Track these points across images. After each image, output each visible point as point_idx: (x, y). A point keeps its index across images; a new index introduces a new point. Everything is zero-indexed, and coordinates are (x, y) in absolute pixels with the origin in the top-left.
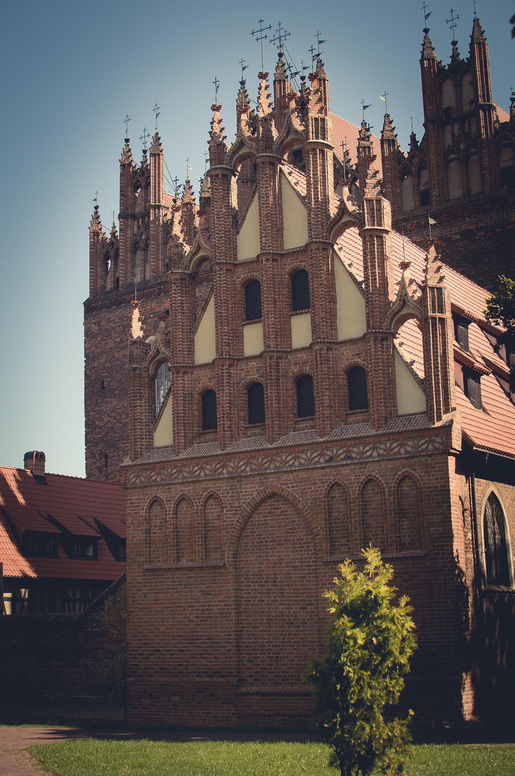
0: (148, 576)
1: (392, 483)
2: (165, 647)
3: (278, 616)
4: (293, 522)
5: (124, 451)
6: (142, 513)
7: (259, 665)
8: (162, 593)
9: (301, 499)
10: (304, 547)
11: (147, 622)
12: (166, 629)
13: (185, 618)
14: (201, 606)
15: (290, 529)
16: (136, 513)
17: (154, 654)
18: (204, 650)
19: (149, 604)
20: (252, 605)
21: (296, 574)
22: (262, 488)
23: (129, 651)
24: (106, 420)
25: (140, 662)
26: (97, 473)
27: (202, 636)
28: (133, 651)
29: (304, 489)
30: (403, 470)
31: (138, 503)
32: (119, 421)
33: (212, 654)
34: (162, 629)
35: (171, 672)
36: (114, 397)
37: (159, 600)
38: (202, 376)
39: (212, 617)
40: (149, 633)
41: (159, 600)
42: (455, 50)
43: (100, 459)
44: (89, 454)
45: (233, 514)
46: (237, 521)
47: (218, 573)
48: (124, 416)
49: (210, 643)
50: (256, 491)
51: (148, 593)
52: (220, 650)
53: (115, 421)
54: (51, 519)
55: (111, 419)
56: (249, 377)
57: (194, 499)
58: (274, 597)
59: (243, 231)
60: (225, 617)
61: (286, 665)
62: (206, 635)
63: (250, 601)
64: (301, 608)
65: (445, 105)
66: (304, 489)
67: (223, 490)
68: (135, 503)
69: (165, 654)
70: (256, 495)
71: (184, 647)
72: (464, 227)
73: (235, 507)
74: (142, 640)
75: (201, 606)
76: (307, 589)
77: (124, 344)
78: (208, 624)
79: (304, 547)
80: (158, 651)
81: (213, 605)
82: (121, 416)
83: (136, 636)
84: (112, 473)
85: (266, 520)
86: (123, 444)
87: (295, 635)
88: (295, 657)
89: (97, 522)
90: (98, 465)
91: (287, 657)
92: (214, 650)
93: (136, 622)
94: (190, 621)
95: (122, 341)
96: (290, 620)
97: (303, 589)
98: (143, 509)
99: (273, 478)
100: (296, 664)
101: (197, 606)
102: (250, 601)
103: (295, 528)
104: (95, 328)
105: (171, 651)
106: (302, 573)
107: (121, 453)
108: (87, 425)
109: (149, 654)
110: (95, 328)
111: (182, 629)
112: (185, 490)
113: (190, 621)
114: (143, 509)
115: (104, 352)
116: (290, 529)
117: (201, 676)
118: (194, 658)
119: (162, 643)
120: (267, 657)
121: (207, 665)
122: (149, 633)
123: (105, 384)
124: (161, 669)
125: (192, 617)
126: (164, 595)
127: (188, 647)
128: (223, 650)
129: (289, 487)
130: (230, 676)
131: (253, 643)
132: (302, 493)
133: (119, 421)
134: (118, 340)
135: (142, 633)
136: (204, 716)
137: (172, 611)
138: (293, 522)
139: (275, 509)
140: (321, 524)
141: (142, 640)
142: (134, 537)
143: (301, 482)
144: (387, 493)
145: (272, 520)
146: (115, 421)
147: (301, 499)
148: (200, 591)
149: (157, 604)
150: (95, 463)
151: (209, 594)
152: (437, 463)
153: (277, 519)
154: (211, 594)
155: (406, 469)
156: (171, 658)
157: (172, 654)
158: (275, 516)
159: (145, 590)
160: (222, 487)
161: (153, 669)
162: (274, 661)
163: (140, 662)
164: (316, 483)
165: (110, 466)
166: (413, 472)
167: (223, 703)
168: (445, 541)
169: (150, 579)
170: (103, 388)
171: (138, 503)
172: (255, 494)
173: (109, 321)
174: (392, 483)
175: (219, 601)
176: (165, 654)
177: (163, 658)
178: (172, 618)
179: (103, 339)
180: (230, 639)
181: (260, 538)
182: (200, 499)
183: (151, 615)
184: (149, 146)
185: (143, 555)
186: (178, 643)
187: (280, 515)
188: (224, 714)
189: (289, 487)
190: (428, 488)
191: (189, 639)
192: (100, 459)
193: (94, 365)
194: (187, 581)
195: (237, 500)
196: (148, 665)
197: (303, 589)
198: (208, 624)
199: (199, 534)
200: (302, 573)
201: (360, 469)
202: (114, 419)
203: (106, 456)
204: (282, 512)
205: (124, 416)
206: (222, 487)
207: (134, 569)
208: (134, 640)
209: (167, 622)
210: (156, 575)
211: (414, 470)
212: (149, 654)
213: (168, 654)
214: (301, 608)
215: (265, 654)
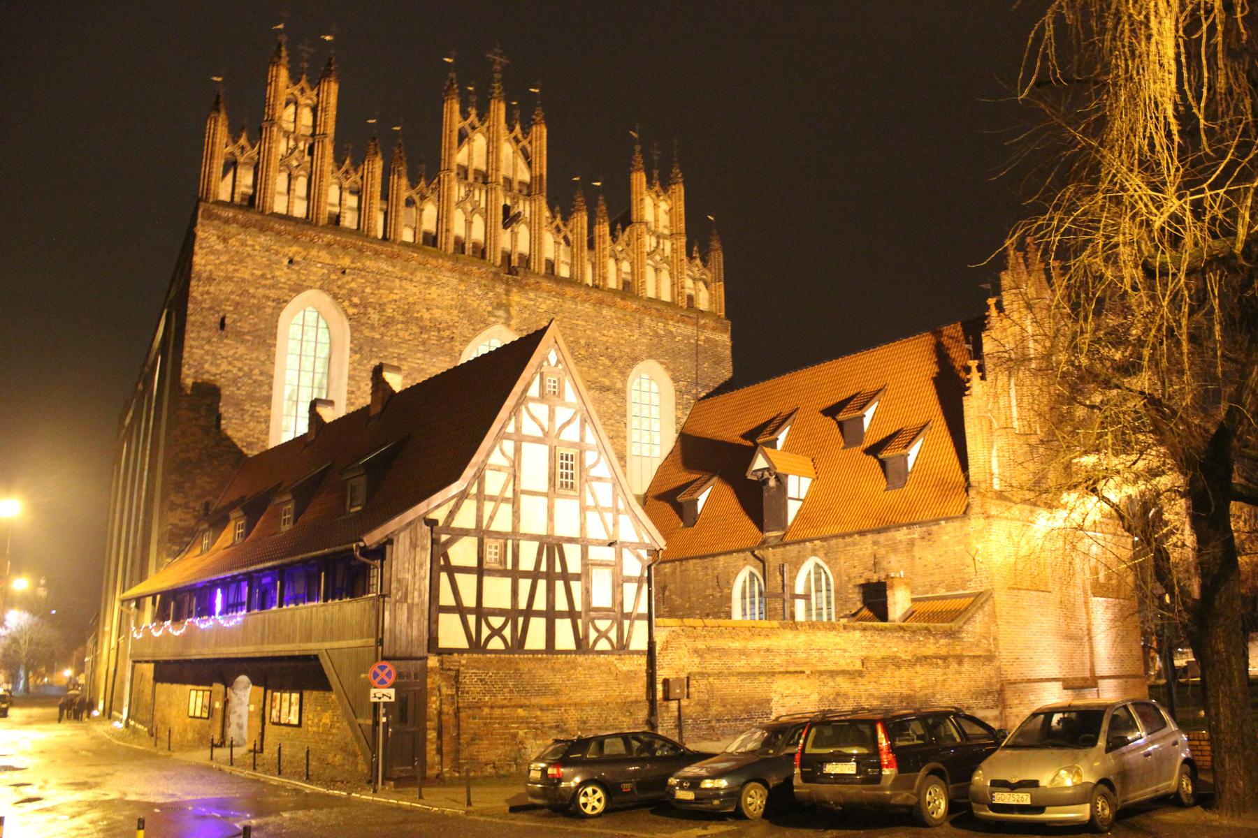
5: (252, 415)
24: (224, 367)
53: (241, 374)
77: (268, 282)
82: (251, 370)
95: (263, 276)
115: (231, 279)
123: (227, 321)
133: (249, 375)
134: (258, 273)
170: (222, 325)
173: (243, 244)
179: (228, 262)
205: (256, 371)
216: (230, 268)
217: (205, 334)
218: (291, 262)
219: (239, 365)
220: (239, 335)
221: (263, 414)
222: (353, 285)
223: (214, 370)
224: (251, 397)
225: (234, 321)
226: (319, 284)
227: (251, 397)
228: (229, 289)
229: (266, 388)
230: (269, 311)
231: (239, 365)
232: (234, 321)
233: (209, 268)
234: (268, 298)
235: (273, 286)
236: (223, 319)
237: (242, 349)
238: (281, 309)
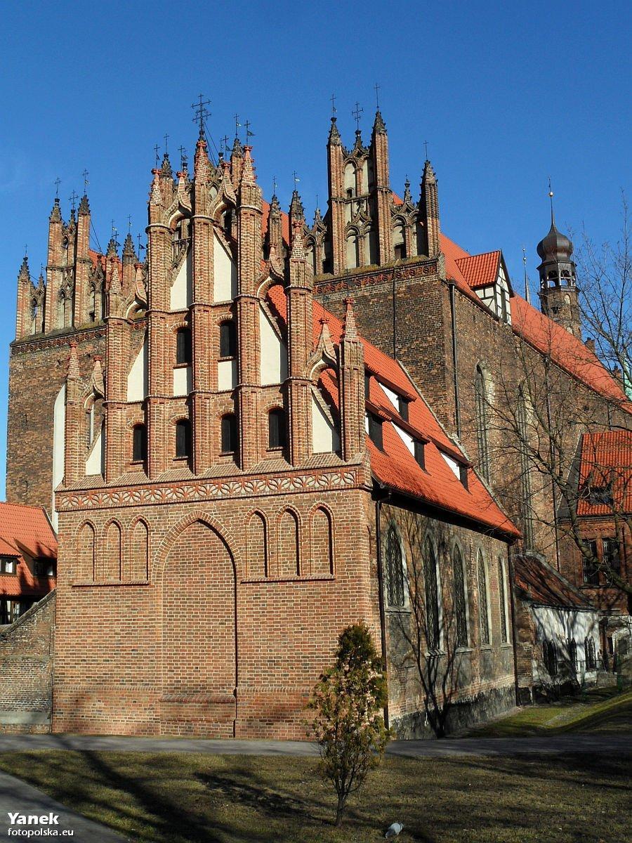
0: (77, 592)
1: (307, 513)
2: (92, 657)
3: (199, 630)
4: (214, 545)
6: (74, 534)
7: (180, 674)
8: (90, 607)
9: (223, 525)
10: (224, 568)
11: (75, 634)
12: (93, 641)
13: (111, 630)
14: (126, 620)
15: (212, 552)
16: (67, 534)
17: (80, 664)
18: (129, 661)
19: (77, 617)
20: (175, 620)
21: (217, 592)
22: (187, 515)
23: (56, 660)
24: (27, 450)
25: (66, 670)
26: (16, 497)
27: (127, 647)
28: (60, 660)
29: (226, 516)
30: (318, 502)
31: (70, 525)
32: (40, 451)
33: (136, 664)
34: (89, 640)
35: (97, 681)
36: (36, 430)
37: (87, 614)
38: (134, 412)
39: (136, 630)
40: (76, 644)
41: (87, 614)
42: (358, 139)
43: (20, 486)
44: (9, 481)
45: (160, 537)
46: (163, 543)
47: (144, 590)
49: (134, 654)
50: (182, 517)
51: (76, 608)
52: (143, 661)
53: (36, 452)
54: (421, 490)
55: (33, 450)
56: (177, 415)
57: (124, 523)
58: (195, 613)
59: (175, 283)
60: (149, 630)
61: (205, 675)
62: (131, 647)
63: (173, 616)
64: (220, 624)
65: (347, 187)
66: (226, 516)
67: (151, 515)
68: (67, 525)
69: (91, 664)
70: (181, 521)
71: (109, 657)
72: (360, 294)
73: (161, 531)
74: (70, 650)
75: (126, 620)
76: (226, 606)
78: (132, 637)
79: (224, 568)
80: (85, 660)
81: (138, 620)
83: (64, 647)
85: (189, 543)
87: (214, 647)
88: (213, 668)
89: (17, 541)
90: (18, 491)
91: (206, 668)
92: (138, 661)
93: (65, 634)
94: (116, 634)
95: (45, 380)
96: (209, 634)
97: (222, 606)
98: (74, 531)
99: (198, 505)
100: (214, 675)
101: (123, 620)
102: (173, 616)
103: (217, 552)
104: (20, 367)
105: (97, 661)
106: (222, 592)
107: (40, 480)
108: (9, 454)
109: (76, 664)
110: (20, 367)
111: (108, 641)
112: (115, 515)
113: (116, 634)
114: (74, 531)
115: (28, 389)
116: (212, 552)
117: (125, 684)
118: (119, 667)
119: (89, 654)
120: (187, 668)
121: (130, 674)
122: (76, 644)
124: (87, 677)
125: (118, 630)
126: (92, 609)
127: (114, 657)
128: (147, 661)
129: (212, 514)
130: (152, 685)
131: (174, 654)
132: (224, 520)
133: (40, 451)
135: (69, 644)
136: (127, 721)
137: (99, 624)
138: (214, 545)
139: (198, 533)
140: (240, 548)
141: (70, 650)
142: (65, 556)
143: (224, 510)
144: (302, 522)
145: (195, 543)
146: (36, 452)
147: (223, 525)
148: (127, 607)
149: (84, 617)
150: (15, 488)
151: (135, 610)
152: (347, 497)
153: (200, 543)
154: (137, 609)
155: (320, 501)
156: (97, 667)
157: (98, 664)
158: (199, 540)
159: (74, 604)
160: (150, 512)
161: (79, 677)
162: (194, 671)
163: (66, 670)
164: (238, 512)
166: (326, 504)
167: (145, 709)
168: (354, 566)
169: (79, 595)
171: (70, 525)
172: (180, 519)
174: (307, 513)
175: (144, 616)
176: (91, 664)
177: (89, 667)
178: (99, 631)
180: (153, 650)
181: (184, 560)
182: (129, 522)
183: (79, 628)
184: (77, 206)
185: (73, 572)
186: (104, 654)
187: (204, 539)
188: (145, 719)
189: (212, 514)
190: (340, 518)
191: (114, 650)
192: (20, 486)
193: (19, 400)
194: (115, 597)
195: (164, 524)
196: (75, 674)
197: (222, 606)
198: (132, 637)
199: (127, 555)
200: (222, 592)
201: (278, 499)
204: (204, 536)
206: (150, 512)
207: (64, 585)
208: (62, 650)
209: (94, 634)
210: (85, 591)
211: (328, 502)
212: (76, 664)
213: (94, 664)
214: (220, 624)
215: (185, 664)
216: (27, 381)
221: (49, 475)
224: (42, 466)
225: (31, 417)
227: (42, 466)
228: (27, 396)
229: (50, 457)
230: (49, 402)
231: (34, 445)
232: (31, 417)
233: (17, 385)
234: (47, 394)
235: (50, 385)
237: (36, 434)
238: (55, 399)
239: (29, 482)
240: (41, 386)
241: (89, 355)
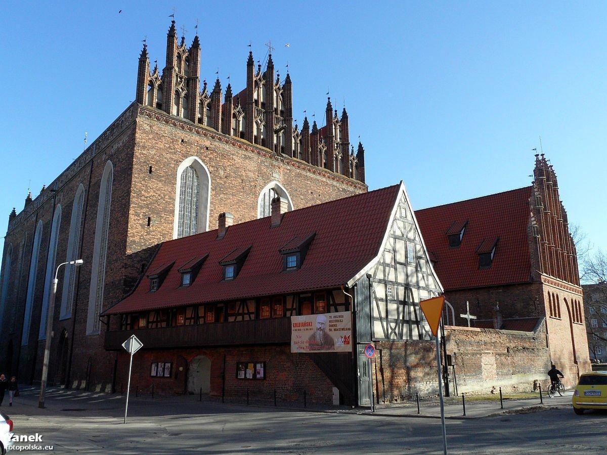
5: (165, 220)
24: (152, 193)
48: (167, 197)
72: (343, 187)
82: (165, 196)
84: (153, 232)
86: (165, 215)
95: (169, 147)
107: (162, 220)
133: (163, 198)
150: (139, 220)
165: (152, 226)
170: (151, 171)
173: (160, 129)
202: (159, 196)
203: (149, 219)
217: (142, 176)
218: (182, 141)
219: (159, 193)
220: (158, 177)
221: (171, 219)
222: (211, 156)
223: (146, 195)
224: (164, 210)
226: (196, 154)
227: (164, 210)
228: (153, 153)
229: (172, 205)
231: (159, 193)
233: (143, 140)
236: (151, 167)
237: (160, 185)
239: (152, 219)
240: (165, 149)
241: (207, 148)
